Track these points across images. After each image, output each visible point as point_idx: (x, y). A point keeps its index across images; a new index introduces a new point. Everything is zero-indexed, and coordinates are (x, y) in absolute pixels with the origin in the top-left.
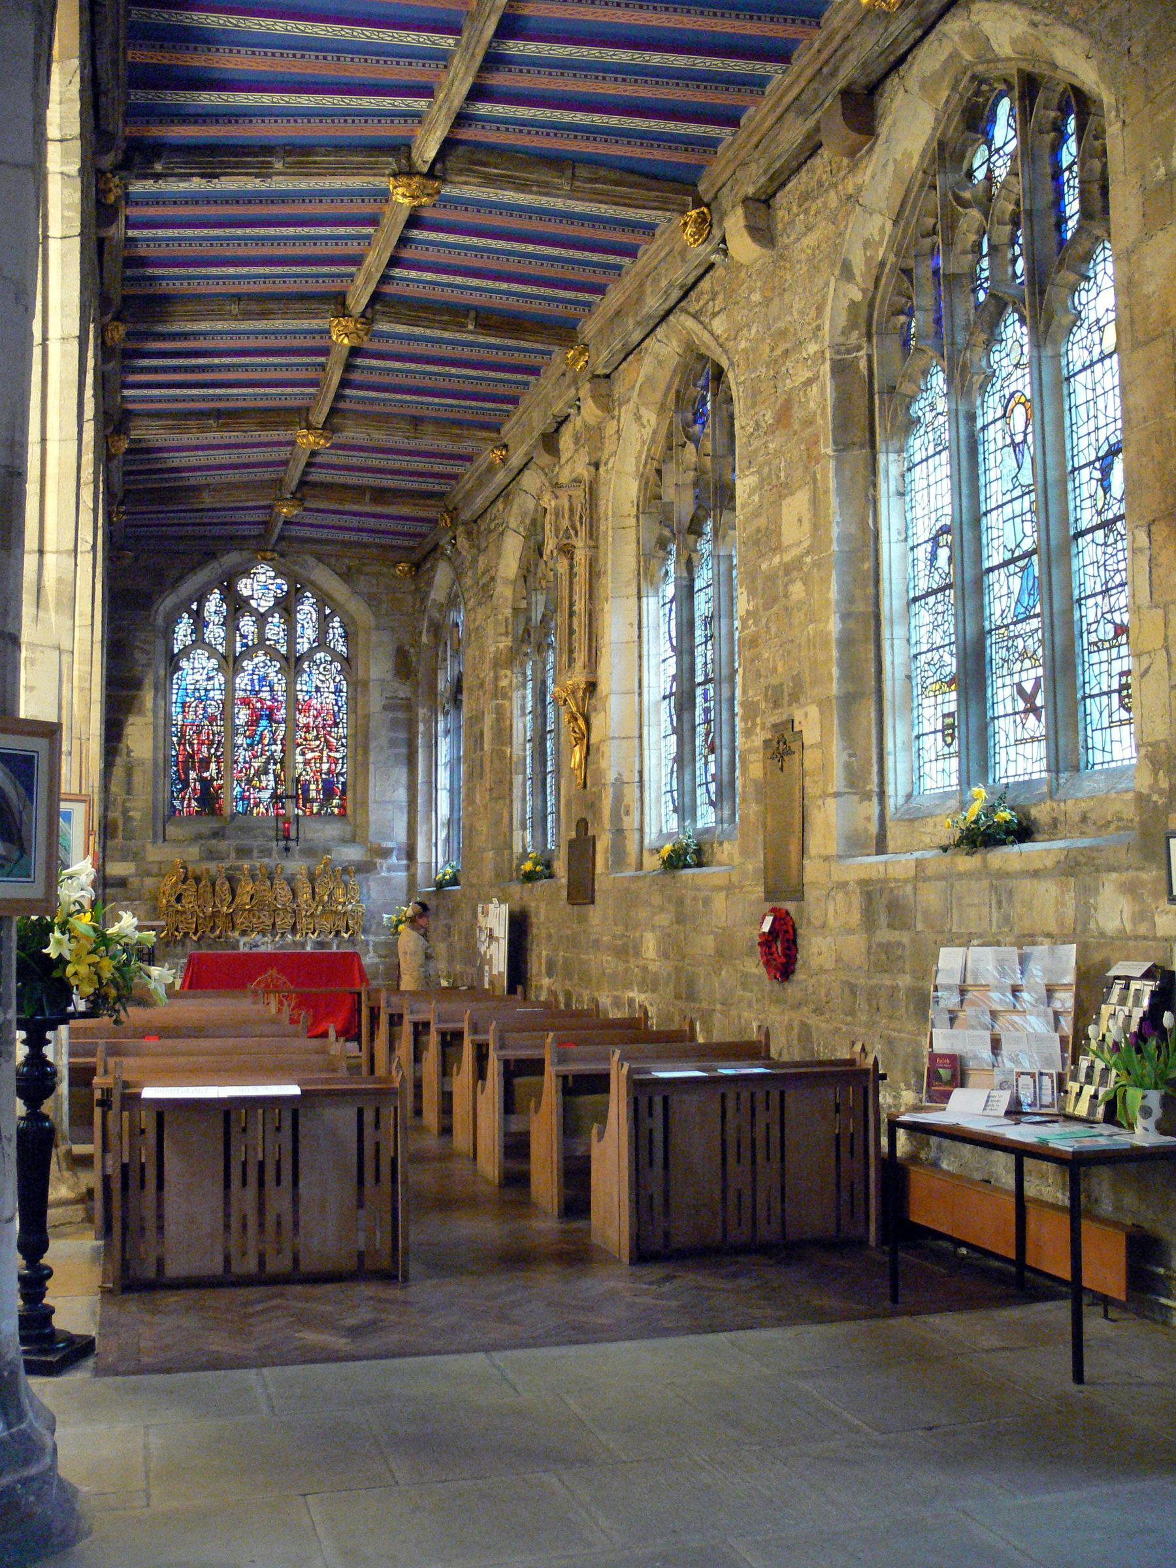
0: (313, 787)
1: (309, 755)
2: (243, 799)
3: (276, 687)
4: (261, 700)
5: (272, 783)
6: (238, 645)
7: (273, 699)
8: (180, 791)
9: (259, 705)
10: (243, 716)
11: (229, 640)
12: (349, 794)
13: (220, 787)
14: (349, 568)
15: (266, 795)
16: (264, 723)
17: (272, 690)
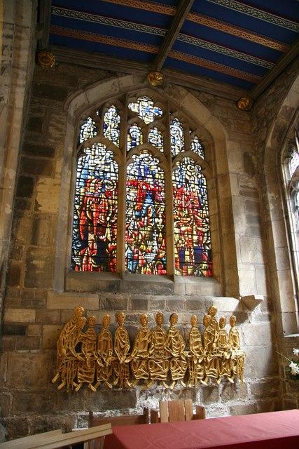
0: (187, 253)
1: (183, 228)
2: (132, 259)
3: (157, 176)
5: (156, 248)
6: (129, 144)
7: (155, 184)
8: (80, 249)
9: (144, 187)
10: (132, 194)
11: (122, 139)
12: (216, 259)
13: (114, 248)
14: (208, 100)
15: (151, 257)
16: (149, 200)
17: (154, 178)
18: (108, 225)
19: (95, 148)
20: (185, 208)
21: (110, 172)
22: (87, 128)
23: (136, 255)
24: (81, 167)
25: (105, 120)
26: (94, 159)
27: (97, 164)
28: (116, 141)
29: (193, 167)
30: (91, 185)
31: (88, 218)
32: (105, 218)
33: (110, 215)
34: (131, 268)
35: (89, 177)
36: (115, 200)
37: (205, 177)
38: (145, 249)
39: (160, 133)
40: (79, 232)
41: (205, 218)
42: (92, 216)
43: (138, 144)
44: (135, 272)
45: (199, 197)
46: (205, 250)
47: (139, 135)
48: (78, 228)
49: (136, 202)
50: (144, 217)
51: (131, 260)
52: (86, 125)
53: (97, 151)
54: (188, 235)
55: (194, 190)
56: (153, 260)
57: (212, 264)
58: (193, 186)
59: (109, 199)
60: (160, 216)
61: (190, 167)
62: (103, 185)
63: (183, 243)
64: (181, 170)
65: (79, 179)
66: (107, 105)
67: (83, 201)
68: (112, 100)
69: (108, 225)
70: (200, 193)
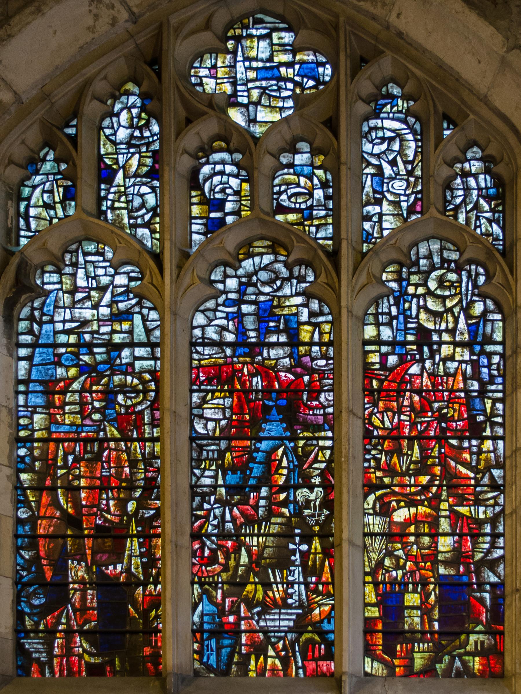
0: (412, 599)
1: (401, 515)
2: (218, 633)
3: (305, 334)
4: (266, 371)
7: (297, 364)
8: (43, 612)
9: (257, 382)
15: (283, 621)
16: (274, 428)
17: (294, 341)
18: (134, 529)
19: (75, 265)
20: (411, 439)
21: (132, 345)
22: (41, 200)
23: (231, 619)
24: (27, 339)
25: (106, 148)
26: (72, 307)
27: (85, 323)
28: (147, 225)
29: (453, 277)
30: (68, 397)
31: (64, 511)
32: (122, 504)
33: (137, 494)
34: (213, 659)
35: (60, 372)
36: (154, 440)
37: (499, 309)
38: (260, 595)
39: (318, 161)
40: (36, 560)
41: (488, 468)
42: (76, 504)
43: (230, 219)
44: (227, 673)
45: (467, 392)
46: (481, 585)
47: (234, 182)
48: (33, 546)
49: (229, 439)
50: (257, 489)
51: (213, 633)
52: (38, 179)
53: (81, 273)
54: (418, 535)
55: (452, 366)
56: (290, 630)
57: (502, 633)
58: (446, 350)
59: (133, 440)
60: (317, 481)
61: (441, 281)
62: (109, 395)
63: (397, 567)
64: (401, 297)
65: (26, 382)
66: (100, 87)
67: (43, 458)
68: (116, 66)
69: (134, 529)
70: (476, 376)
